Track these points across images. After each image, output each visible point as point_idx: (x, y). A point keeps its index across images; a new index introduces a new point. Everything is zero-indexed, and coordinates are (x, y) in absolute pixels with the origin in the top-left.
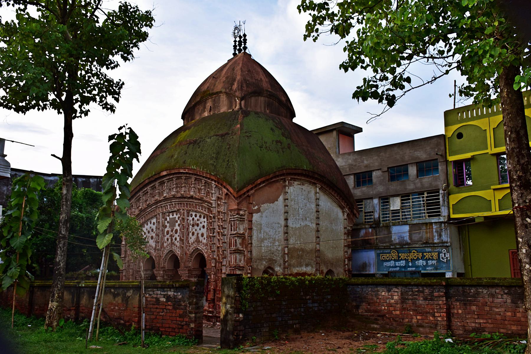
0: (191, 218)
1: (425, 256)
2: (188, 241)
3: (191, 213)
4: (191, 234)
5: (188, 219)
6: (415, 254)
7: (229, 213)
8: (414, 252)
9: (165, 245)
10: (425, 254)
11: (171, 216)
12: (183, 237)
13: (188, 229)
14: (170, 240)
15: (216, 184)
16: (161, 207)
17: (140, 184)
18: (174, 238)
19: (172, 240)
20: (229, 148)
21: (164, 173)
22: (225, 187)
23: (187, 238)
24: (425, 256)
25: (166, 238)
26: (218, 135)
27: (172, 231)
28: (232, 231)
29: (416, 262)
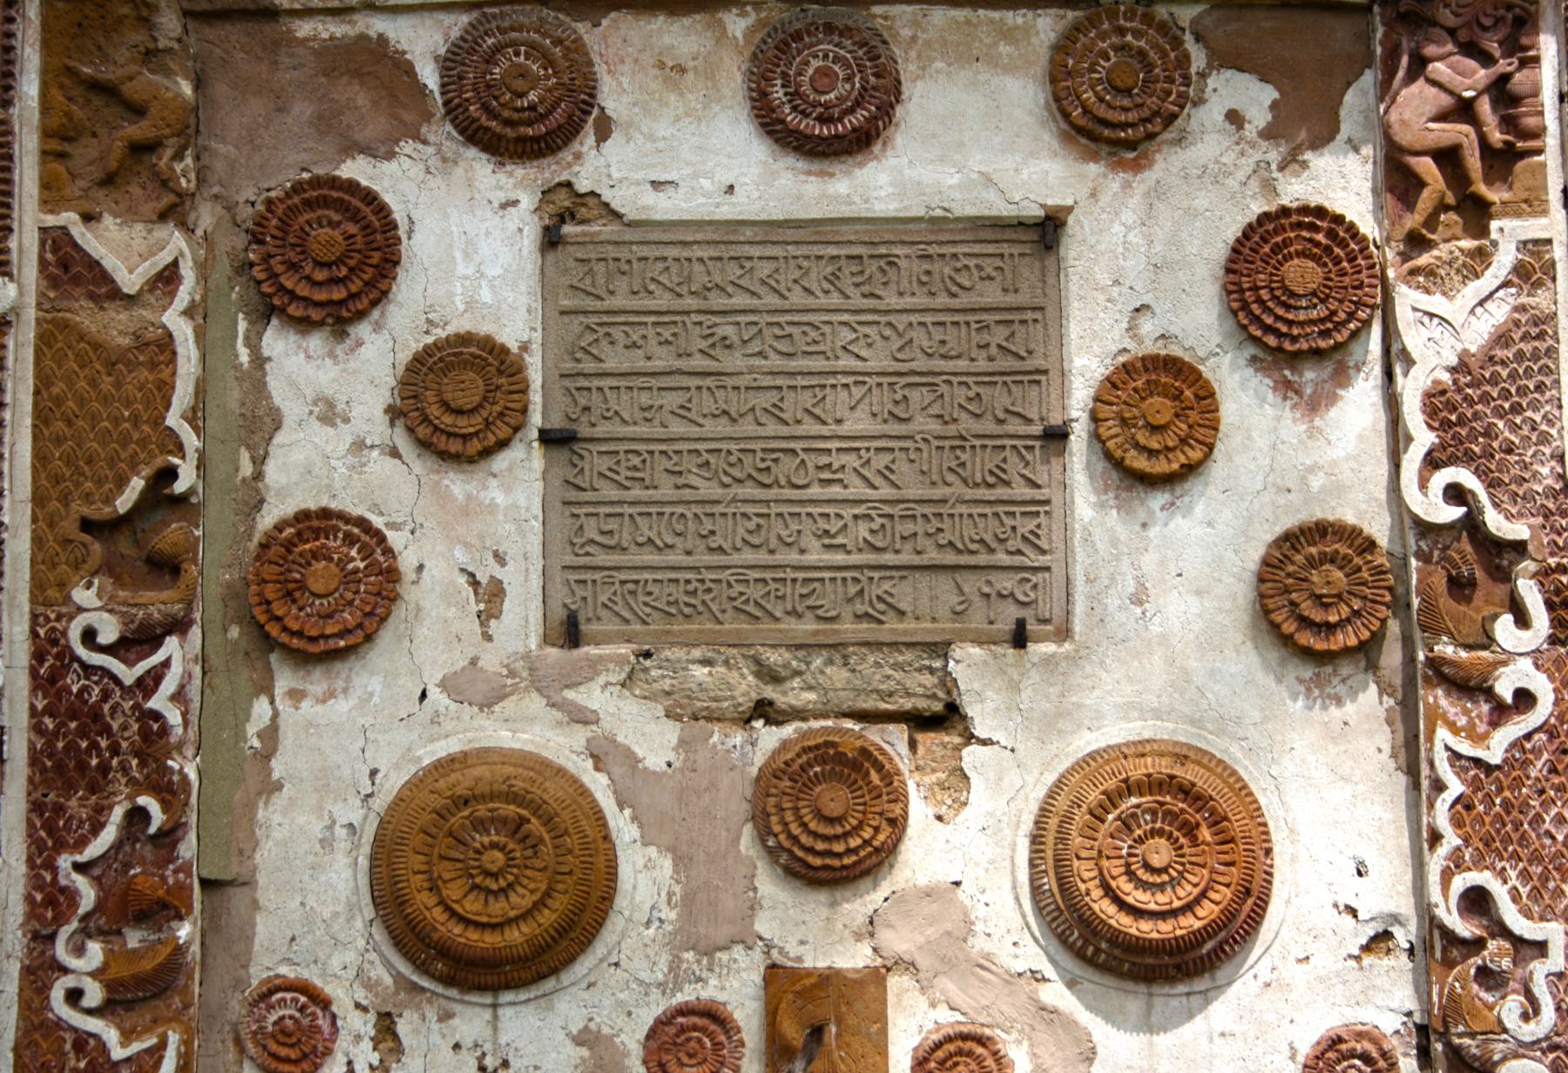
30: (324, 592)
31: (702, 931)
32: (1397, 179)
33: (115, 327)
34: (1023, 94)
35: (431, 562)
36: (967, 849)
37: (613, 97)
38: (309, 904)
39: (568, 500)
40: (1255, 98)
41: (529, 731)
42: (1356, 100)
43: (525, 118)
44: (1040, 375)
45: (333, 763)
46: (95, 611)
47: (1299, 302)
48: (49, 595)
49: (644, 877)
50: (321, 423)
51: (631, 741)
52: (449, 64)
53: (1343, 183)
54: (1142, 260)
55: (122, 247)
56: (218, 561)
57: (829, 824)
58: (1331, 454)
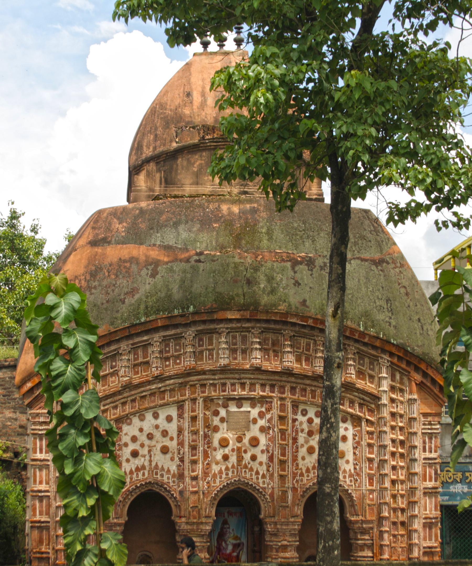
0: (305, 419)
1: (467, 478)
2: (297, 465)
3: (301, 407)
4: (303, 451)
5: (294, 420)
6: (450, 474)
7: (422, 419)
8: (447, 471)
9: (215, 468)
10: (467, 474)
11: (233, 408)
12: (283, 454)
13: (295, 440)
14: (233, 459)
15: (395, 360)
16: (203, 386)
17: (133, 326)
18: (247, 457)
19: (240, 459)
20: (407, 294)
21: (230, 315)
22: (417, 369)
23: (295, 459)
24: (467, 478)
25: (219, 456)
26: (366, 260)
27: (239, 440)
28: (424, 450)
29: (451, 487)
30: (216, 429)
31: (234, 444)
32: (266, 409)
33: (207, 417)
34: (249, 405)
35: (221, 427)
36: (246, 441)
37: (230, 405)
38: (216, 443)
39: (227, 425)
40: (259, 405)
41: (225, 435)
42: (264, 405)
43: (225, 406)
44: (249, 418)
45: (217, 437)
46: (206, 430)
47: (261, 415)
48: (204, 429)
49: (231, 442)
50: (216, 421)
51: (231, 436)
52: (222, 404)
53: (263, 410)
54: (255, 412)
55: (207, 413)
56: (212, 427)
57: (239, 440)
58: (262, 423)
